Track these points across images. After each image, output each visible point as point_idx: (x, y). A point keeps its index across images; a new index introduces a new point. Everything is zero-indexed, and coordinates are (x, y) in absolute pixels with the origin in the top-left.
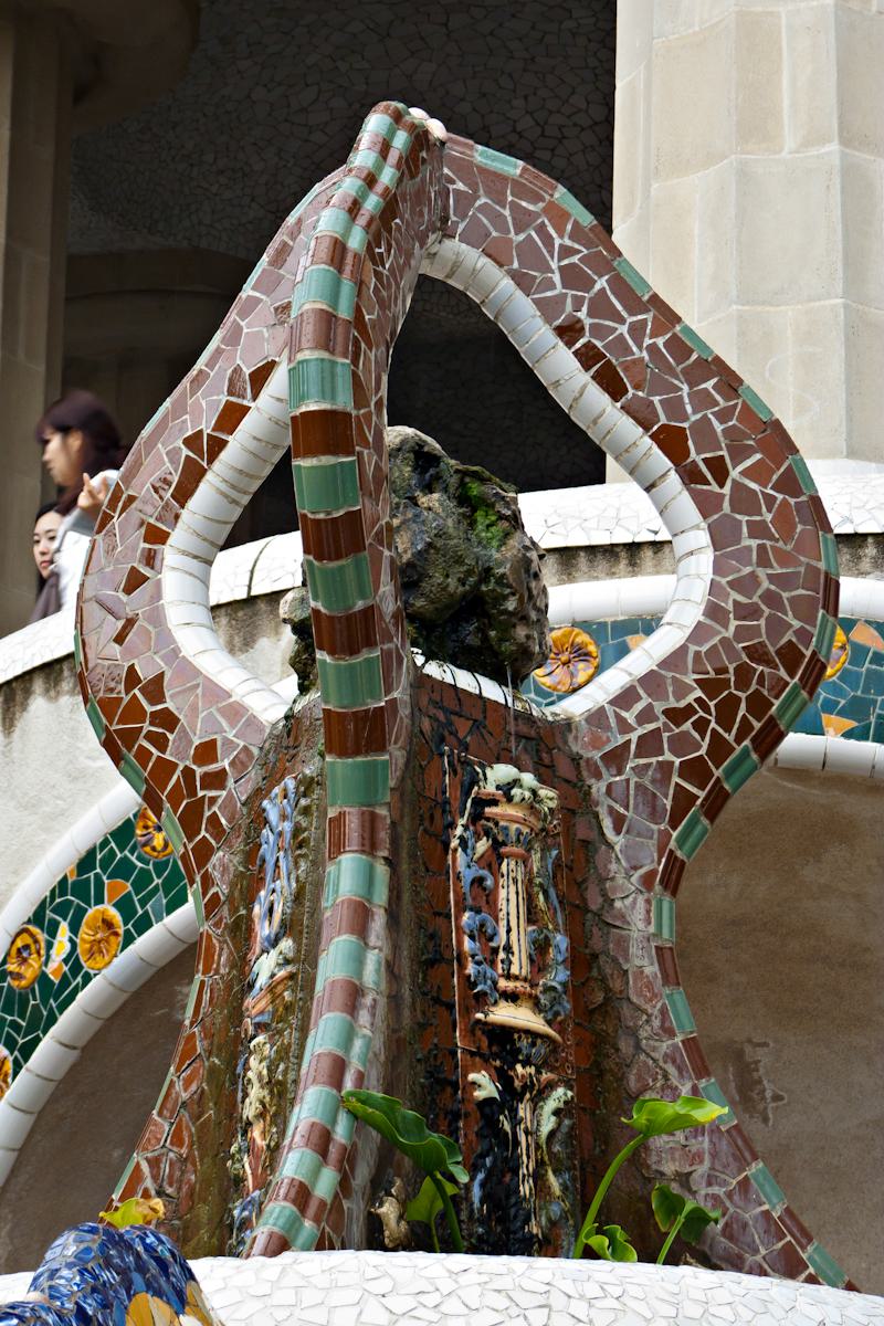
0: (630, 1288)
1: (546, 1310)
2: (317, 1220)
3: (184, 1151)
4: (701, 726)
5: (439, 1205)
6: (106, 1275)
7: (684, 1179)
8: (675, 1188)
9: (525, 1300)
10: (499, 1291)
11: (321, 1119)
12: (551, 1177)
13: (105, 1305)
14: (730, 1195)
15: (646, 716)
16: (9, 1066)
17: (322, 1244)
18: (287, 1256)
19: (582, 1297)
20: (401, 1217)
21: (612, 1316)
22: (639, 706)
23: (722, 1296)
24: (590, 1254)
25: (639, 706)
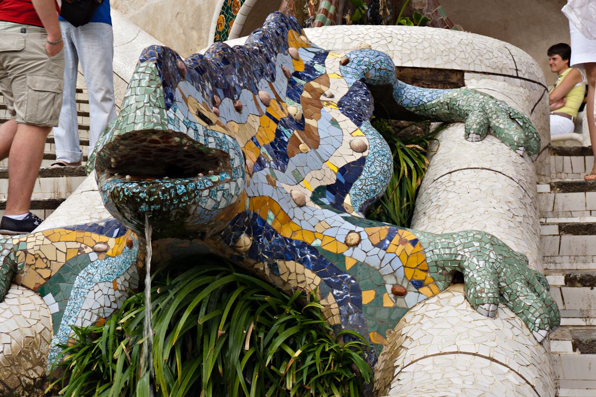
0: (413, 32)
1: (391, 38)
2: (330, 18)
3: (292, 9)
5: (360, 16)
6: (282, 24)
7: (421, 10)
8: (419, 12)
9: (386, 35)
10: (379, 33)
11: (324, 6)
12: (387, 10)
13: (283, 31)
14: (433, 14)
16: (240, 4)
17: (332, 24)
18: (323, 27)
19: (400, 34)
20: (350, 20)
21: (408, 39)
23: (436, 33)
24: (400, 24)
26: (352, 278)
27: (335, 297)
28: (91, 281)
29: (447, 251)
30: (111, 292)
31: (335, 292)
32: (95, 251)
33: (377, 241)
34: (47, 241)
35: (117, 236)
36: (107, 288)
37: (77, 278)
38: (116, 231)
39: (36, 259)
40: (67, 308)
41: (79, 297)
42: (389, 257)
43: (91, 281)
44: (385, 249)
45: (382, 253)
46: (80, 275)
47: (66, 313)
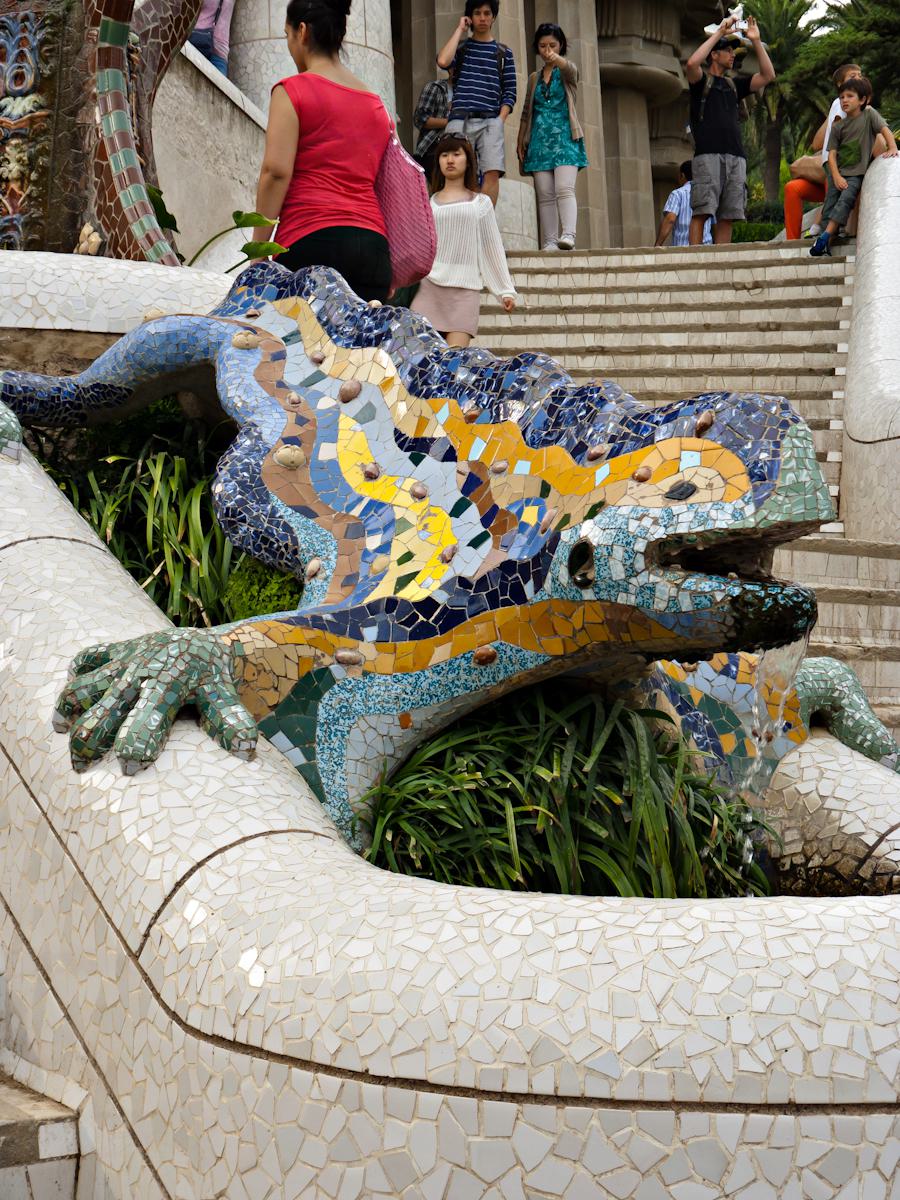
4: (170, 27)
15: (154, 19)
22: (152, 13)
25: (152, 13)
26: (705, 717)
27: (698, 744)
28: (347, 713)
29: (822, 685)
30: (397, 731)
31: (696, 736)
32: (339, 662)
33: (720, 668)
34: (272, 644)
35: (381, 639)
36: (389, 724)
37: (320, 707)
38: (371, 633)
39: (259, 672)
40: (318, 756)
41: (334, 739)
42: (743, 689)
43: (347, 713)
44: (734, 678)
45: (731, 683)
46: (325, 702)
47: (321, 765)
